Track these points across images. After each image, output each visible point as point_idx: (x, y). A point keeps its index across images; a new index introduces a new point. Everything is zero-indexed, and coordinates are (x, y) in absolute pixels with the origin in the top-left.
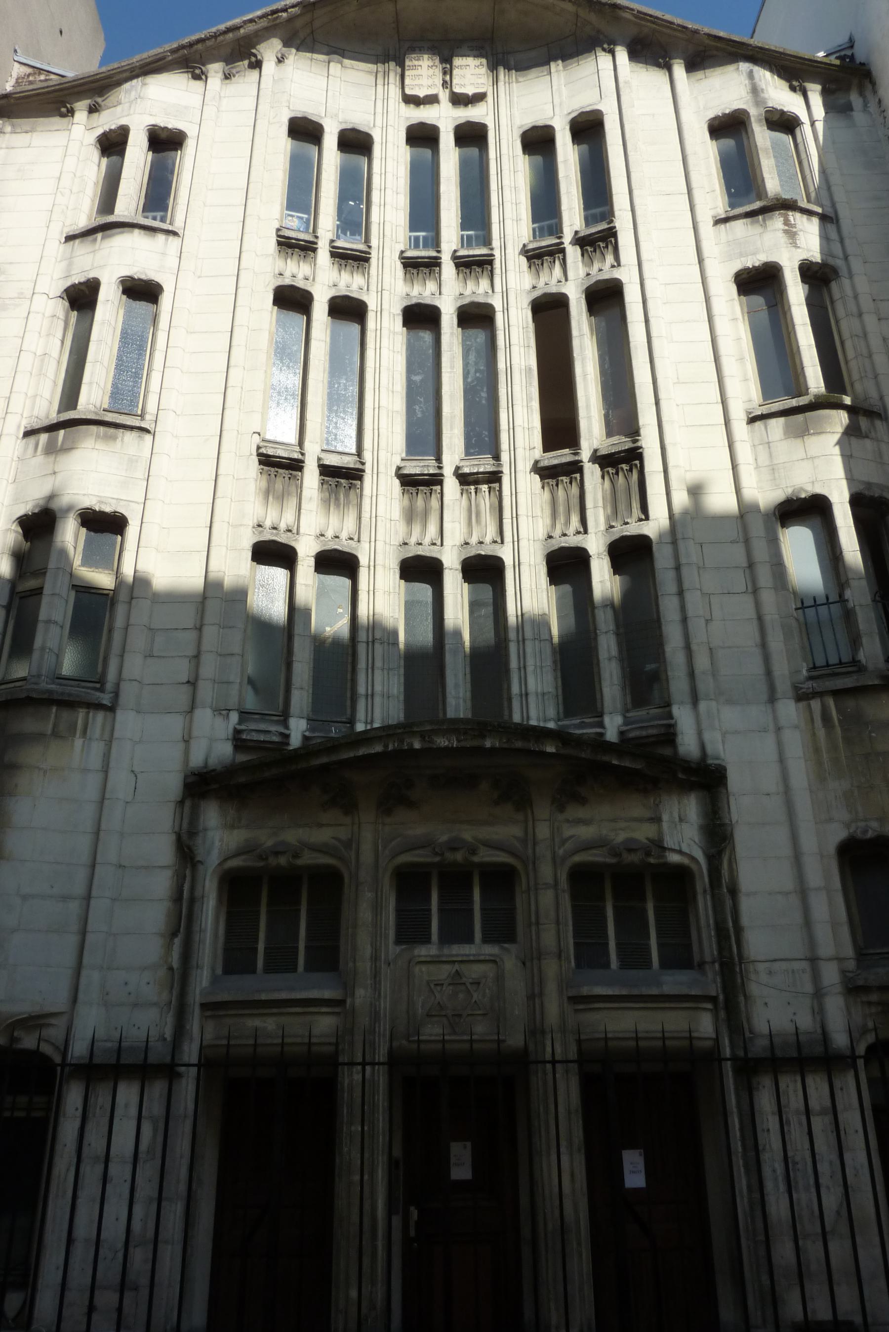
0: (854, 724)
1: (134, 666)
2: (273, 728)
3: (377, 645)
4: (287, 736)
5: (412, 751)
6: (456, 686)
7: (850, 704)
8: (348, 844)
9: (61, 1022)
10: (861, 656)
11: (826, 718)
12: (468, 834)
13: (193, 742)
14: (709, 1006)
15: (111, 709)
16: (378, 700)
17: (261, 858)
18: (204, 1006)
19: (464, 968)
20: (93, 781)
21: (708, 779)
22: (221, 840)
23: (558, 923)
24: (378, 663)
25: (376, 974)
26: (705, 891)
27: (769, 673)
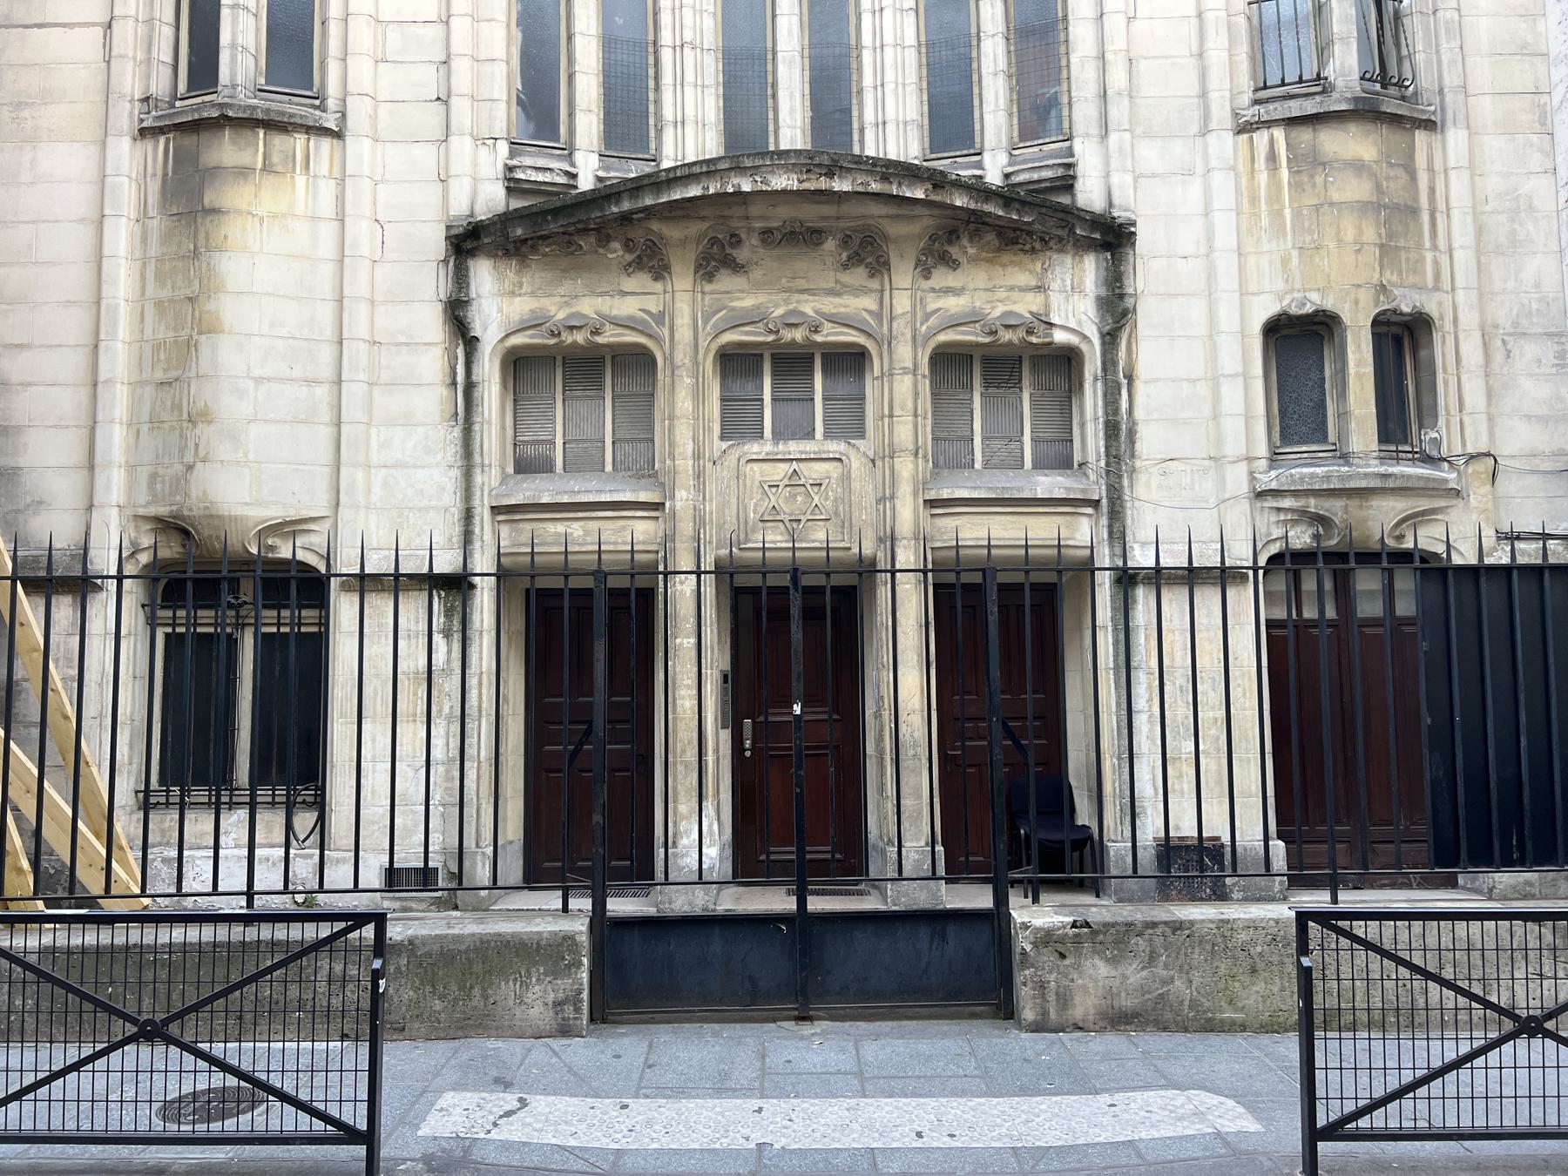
0: (1307, 164)
1: (362, 72)
2: (555, 165)
3: (686, 50)
4: (574, 176)
5: (738, 193)
6: (792, 111)
7: (1304, 135)
8: (659, 318)
9: (323, 528)
10: (1329, 72)
11: (1272, 157)
12: (808, 309)
13: (451, 181)
14: (1089, 510)
15: (338, 135)
16: (689, 129)
17: (553, 334)
18: (496, 510)
19: (803, 468)
20: (328, 231)
21: (1112, 237)
22: (500, 310)
23: (916, 415)
24: (690, 77)
25: (699, 475)
26: (1096, 379)
27: (1204, 94)
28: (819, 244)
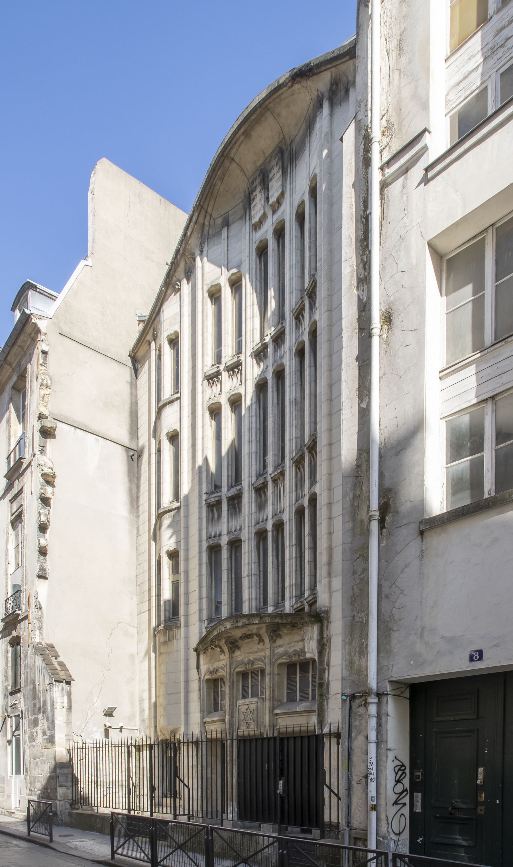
28: (252, 638)
